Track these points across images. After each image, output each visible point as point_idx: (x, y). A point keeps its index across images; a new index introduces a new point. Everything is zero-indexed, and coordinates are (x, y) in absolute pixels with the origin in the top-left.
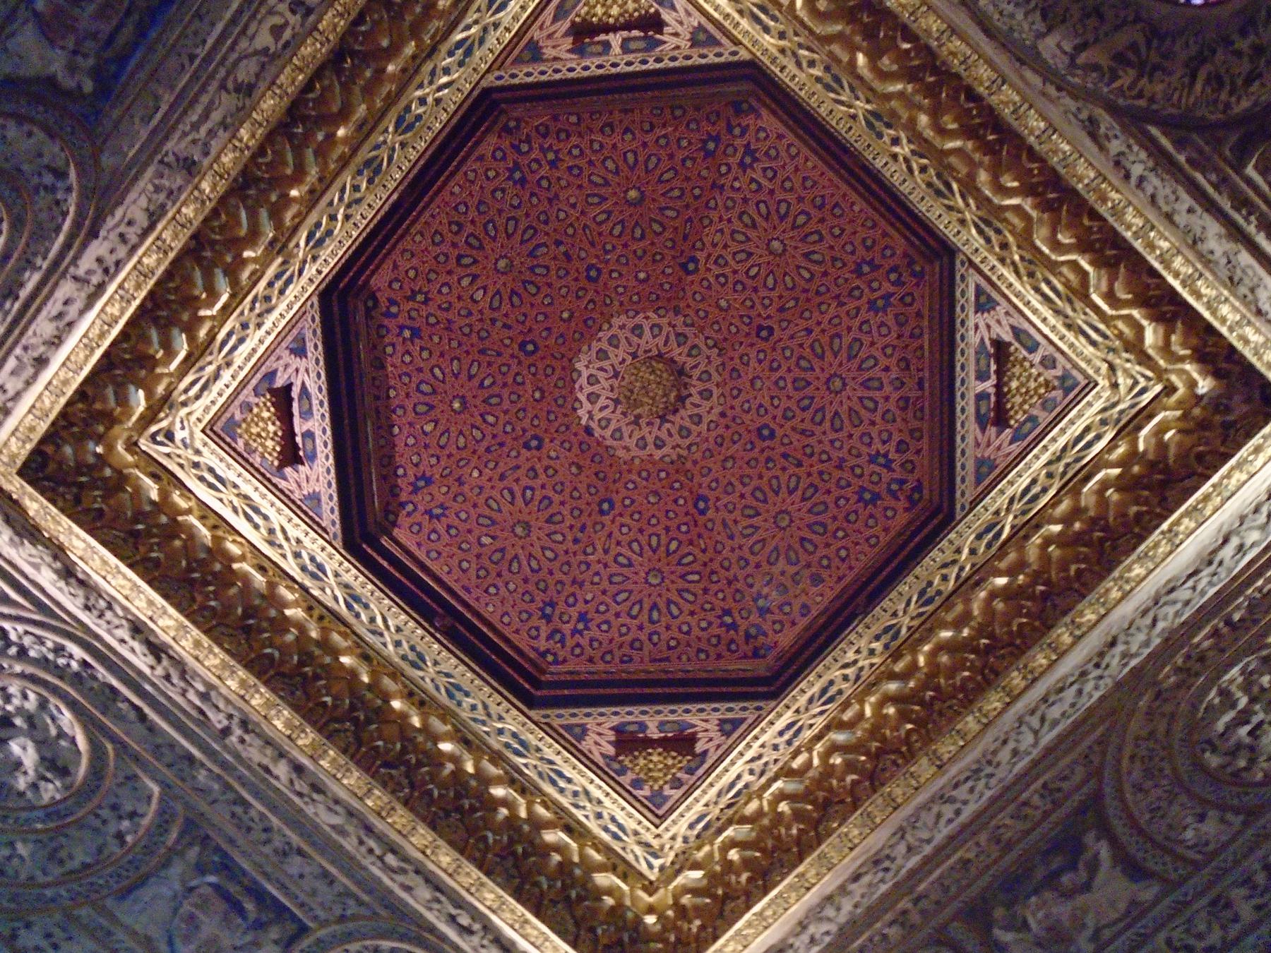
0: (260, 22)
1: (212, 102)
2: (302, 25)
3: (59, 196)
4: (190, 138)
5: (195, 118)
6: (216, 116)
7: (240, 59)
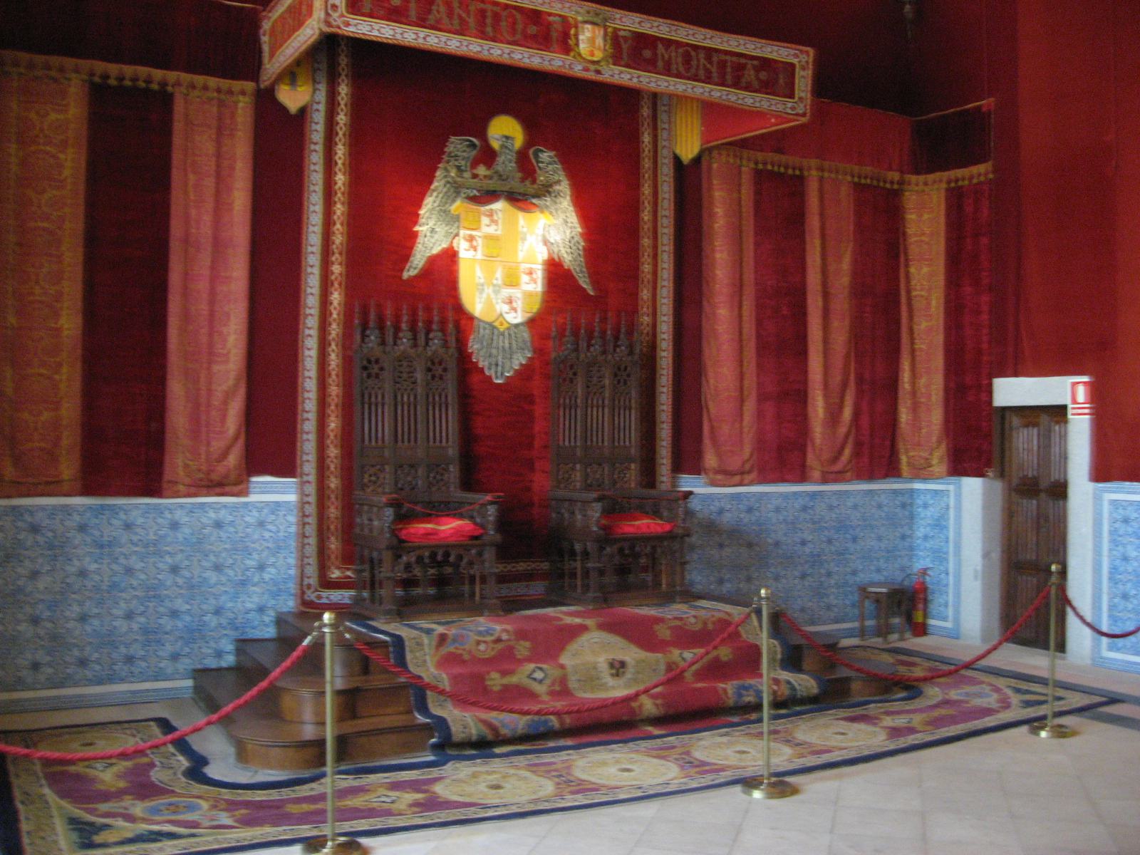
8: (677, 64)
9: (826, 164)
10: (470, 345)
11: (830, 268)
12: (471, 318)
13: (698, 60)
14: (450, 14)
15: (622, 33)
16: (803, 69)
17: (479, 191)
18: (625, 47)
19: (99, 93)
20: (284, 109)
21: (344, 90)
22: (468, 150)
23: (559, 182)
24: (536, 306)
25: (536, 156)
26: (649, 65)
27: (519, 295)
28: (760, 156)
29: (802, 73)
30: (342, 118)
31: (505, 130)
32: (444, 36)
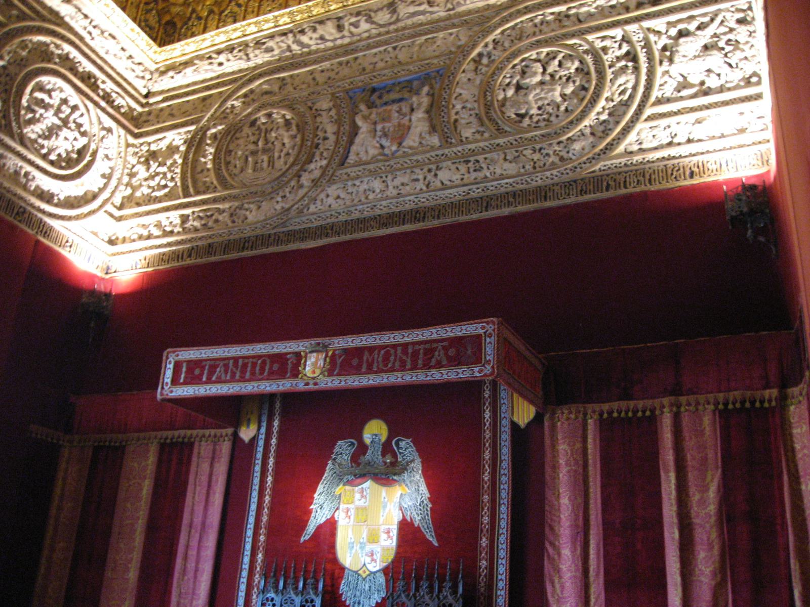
0: (359, 35)
1: (408, 18)
2: (346, 16)
3: (491, 47)
4: (431, 9)
5: (421, 17)
6: (412, 9)
7: (381, 26)
8: (378, 362)
9: (683, 399)
10: (341, 588)
11: (692, 499)
12: (342, 569)
13: (396, 356)
14: (226, 372)
15: (337, 352)
16: (490, 336)
17: (355, 476)
18: (339, 361)
19: (165, 448)
20: (242, 441)
21: (276, 423)
22: (349, 448)
23: (413, 461)
24: (390, 557)
25: (397, 444)
26: (358, 371)
27: (379, 549)
28: (606, 407)
29: (488, 340)
30: (274, 441)
31: (375, 431)
32: (219, 386)
